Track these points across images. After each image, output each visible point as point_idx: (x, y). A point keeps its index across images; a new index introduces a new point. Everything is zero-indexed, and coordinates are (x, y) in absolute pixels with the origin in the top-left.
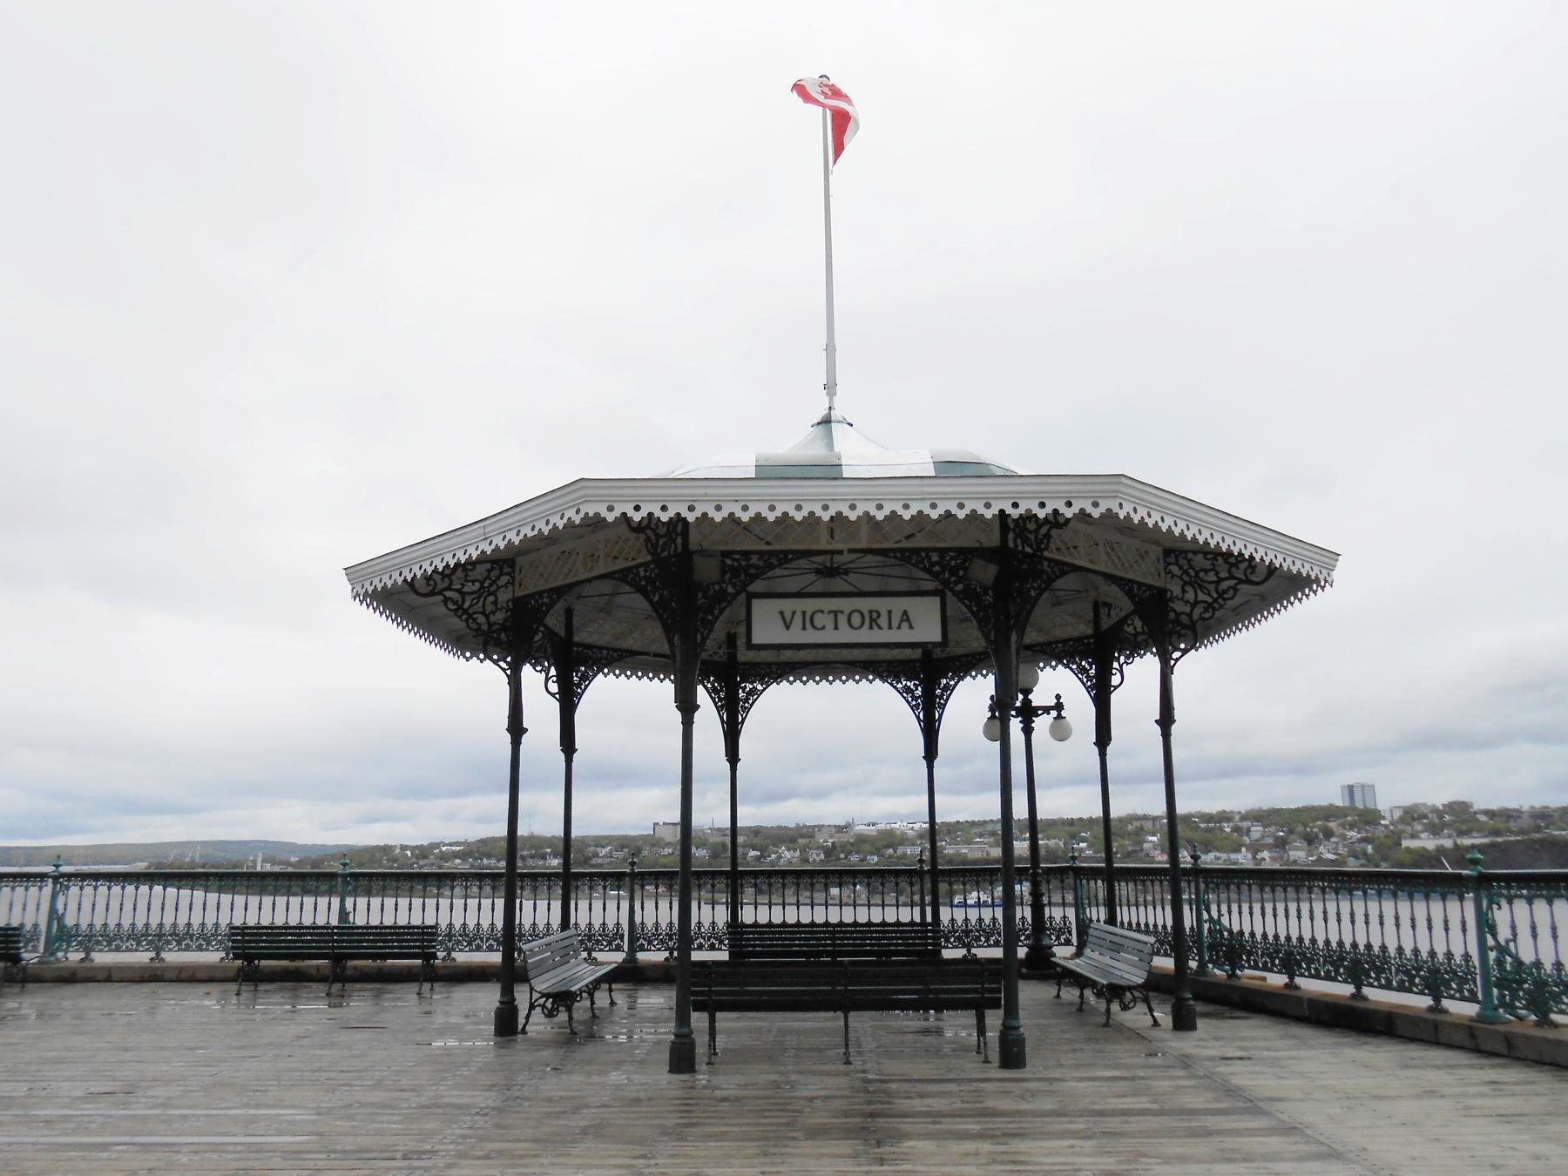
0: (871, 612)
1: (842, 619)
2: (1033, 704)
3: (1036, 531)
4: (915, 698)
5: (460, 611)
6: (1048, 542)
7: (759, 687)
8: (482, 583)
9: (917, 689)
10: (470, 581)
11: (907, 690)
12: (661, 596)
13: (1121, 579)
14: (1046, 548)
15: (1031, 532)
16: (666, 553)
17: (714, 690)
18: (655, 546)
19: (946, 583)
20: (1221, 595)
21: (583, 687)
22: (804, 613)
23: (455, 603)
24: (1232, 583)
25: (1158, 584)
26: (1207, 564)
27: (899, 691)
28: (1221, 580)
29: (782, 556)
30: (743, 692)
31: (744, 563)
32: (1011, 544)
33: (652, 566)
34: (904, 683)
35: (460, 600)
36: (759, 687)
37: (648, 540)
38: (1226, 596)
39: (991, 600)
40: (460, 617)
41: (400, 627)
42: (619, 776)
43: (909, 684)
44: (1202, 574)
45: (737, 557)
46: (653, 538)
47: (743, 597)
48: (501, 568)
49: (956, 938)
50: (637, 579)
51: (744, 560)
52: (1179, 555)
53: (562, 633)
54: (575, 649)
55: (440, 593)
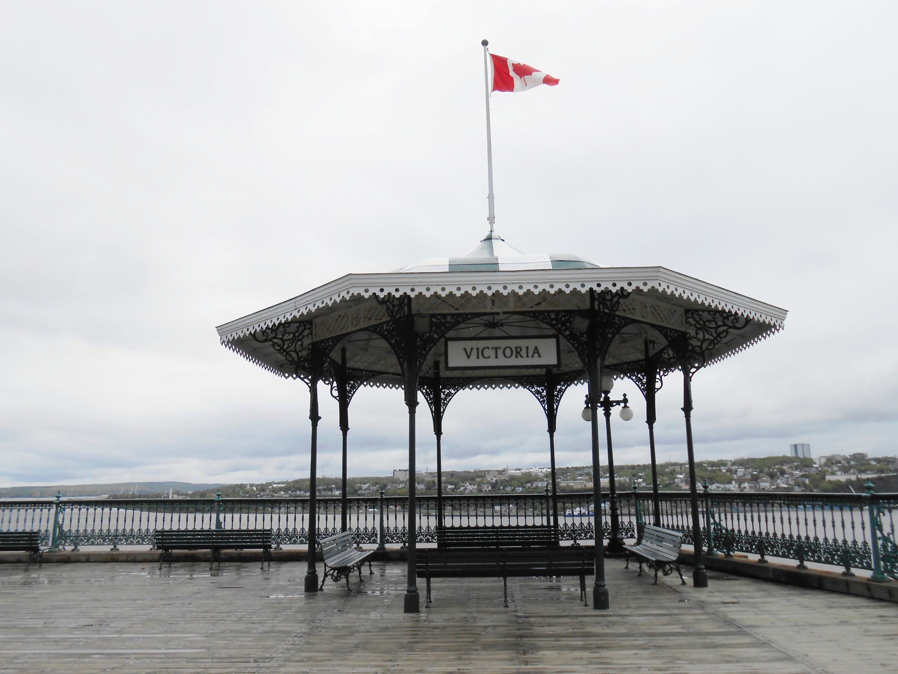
0: (516, 348)
1: (500, 352)
2: (610, 400)
3: (611, 300)
4: (542, 397)
5: (282, 350)
6: (618, 306)
7: (453, 392)
8: (294, 334)
9: (543, 392)
10: (287, 333)
11: (538, 392)
12: (396, 340)
13: (661, 327)
14: (617, 309)
15: (608, 300)
16: (398, 316)
17: (427, 393)
18: (392, 312)
19: (559, 330)
20: (718, 335)
21: (352, 393)
22: (478, 349)
23: (279, 346)
25: (683, 329)
26: (710, 318)
27: (533, 393)
28: (718, 327)
29: (465, 316)
30: (444, 394)
31: (443, 321)
32: (597, 308)
33: (390, 323)
34: (536, 388)
35: (282, 344)
36: (453, 392)
37: (388, 308)
38: (721, 336)
39: (586, 340)
40: (282, 354)
41: (248, 360)
42: (375, 443)
43: (538, 389)
44: (707, 323)
45: (439, 317)
46: (391, 307)
47: (443, 340)
48: (305, 326)
49: (568, 534)
50: (382, 331)
51: (443, 319)
52: (694, 313)
53: (340, 362)
54: (347, 371)
55: (270, 340)
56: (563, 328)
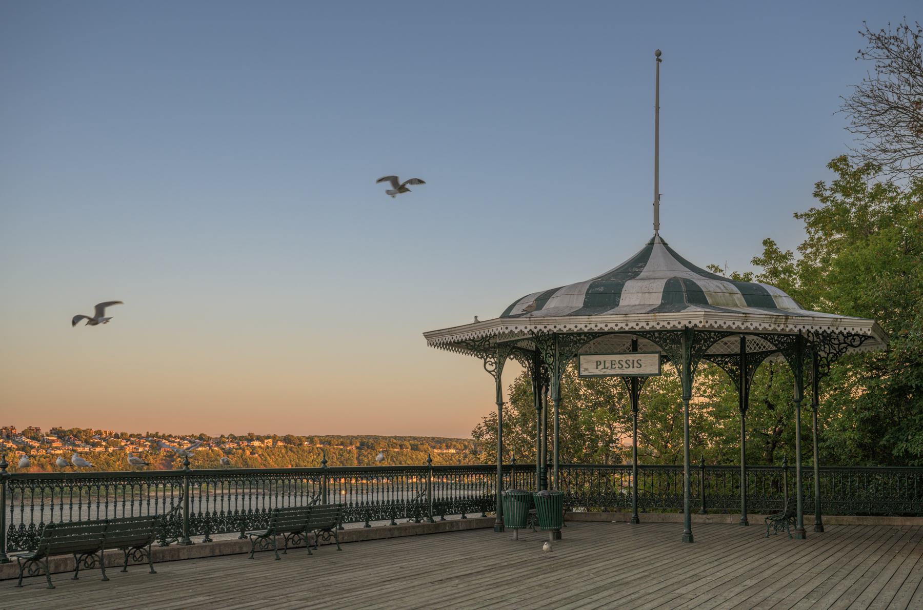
20: (840, 351)
24: (845, 345)
28: (840, 344)
31: (578, 338)
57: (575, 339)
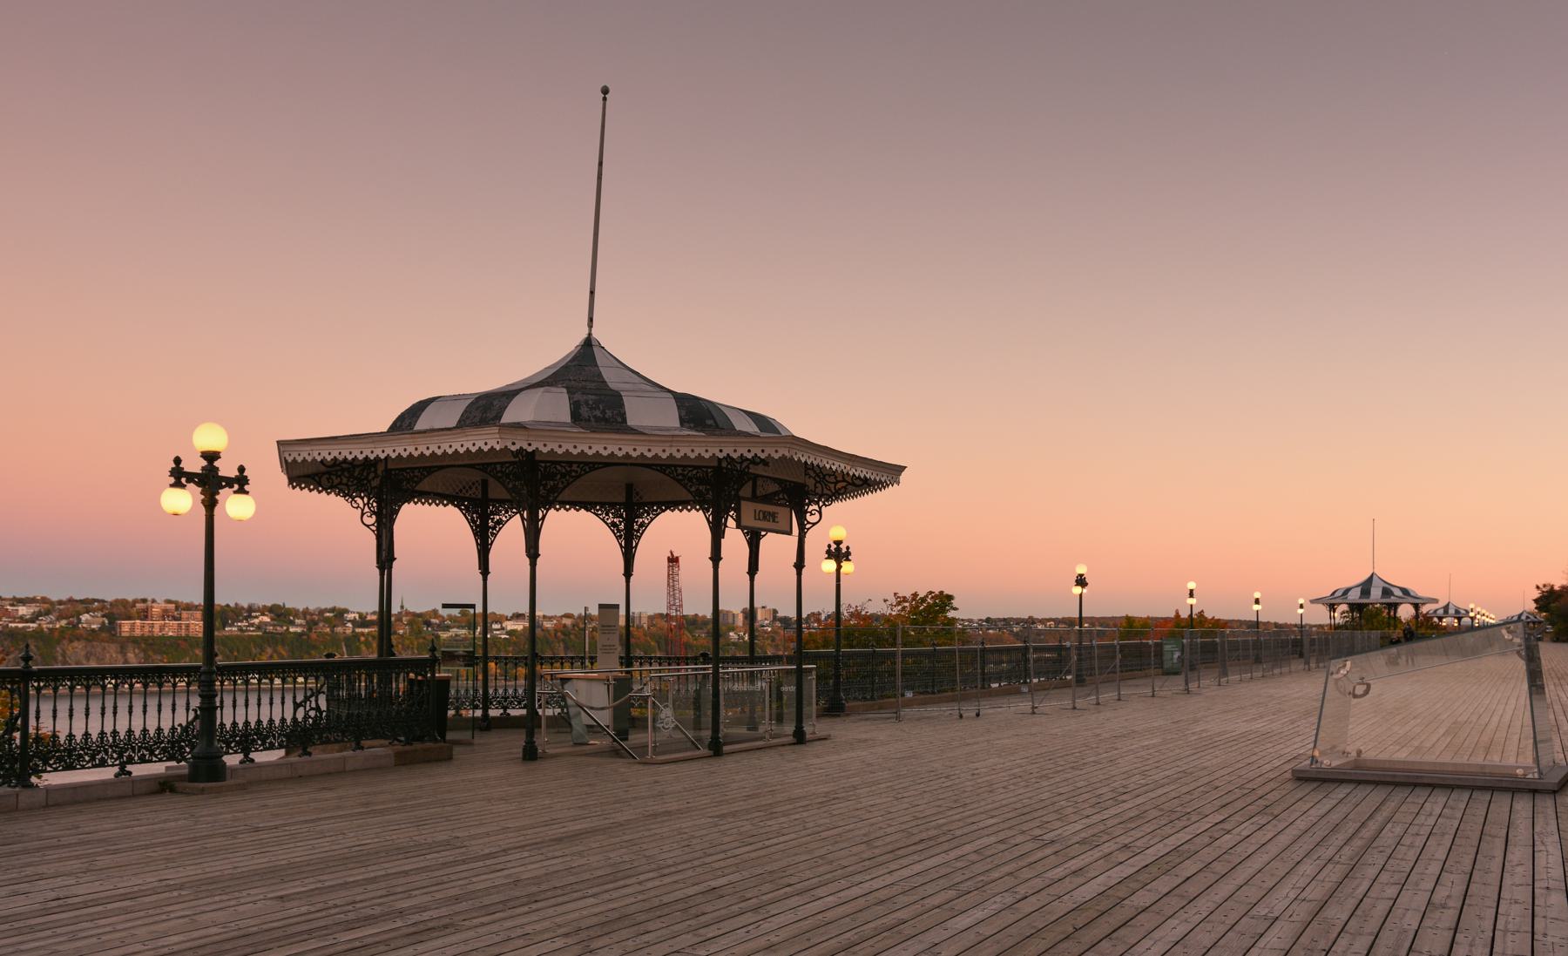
4: (619, 531)
11: (614, 524)
24: (844, 484)
25: (800, 480)
28: (838, 482)
31: (569, 469)
36: (504, 519)
43: (615, 520)
56: (689, 484)
57: (564, 471)
